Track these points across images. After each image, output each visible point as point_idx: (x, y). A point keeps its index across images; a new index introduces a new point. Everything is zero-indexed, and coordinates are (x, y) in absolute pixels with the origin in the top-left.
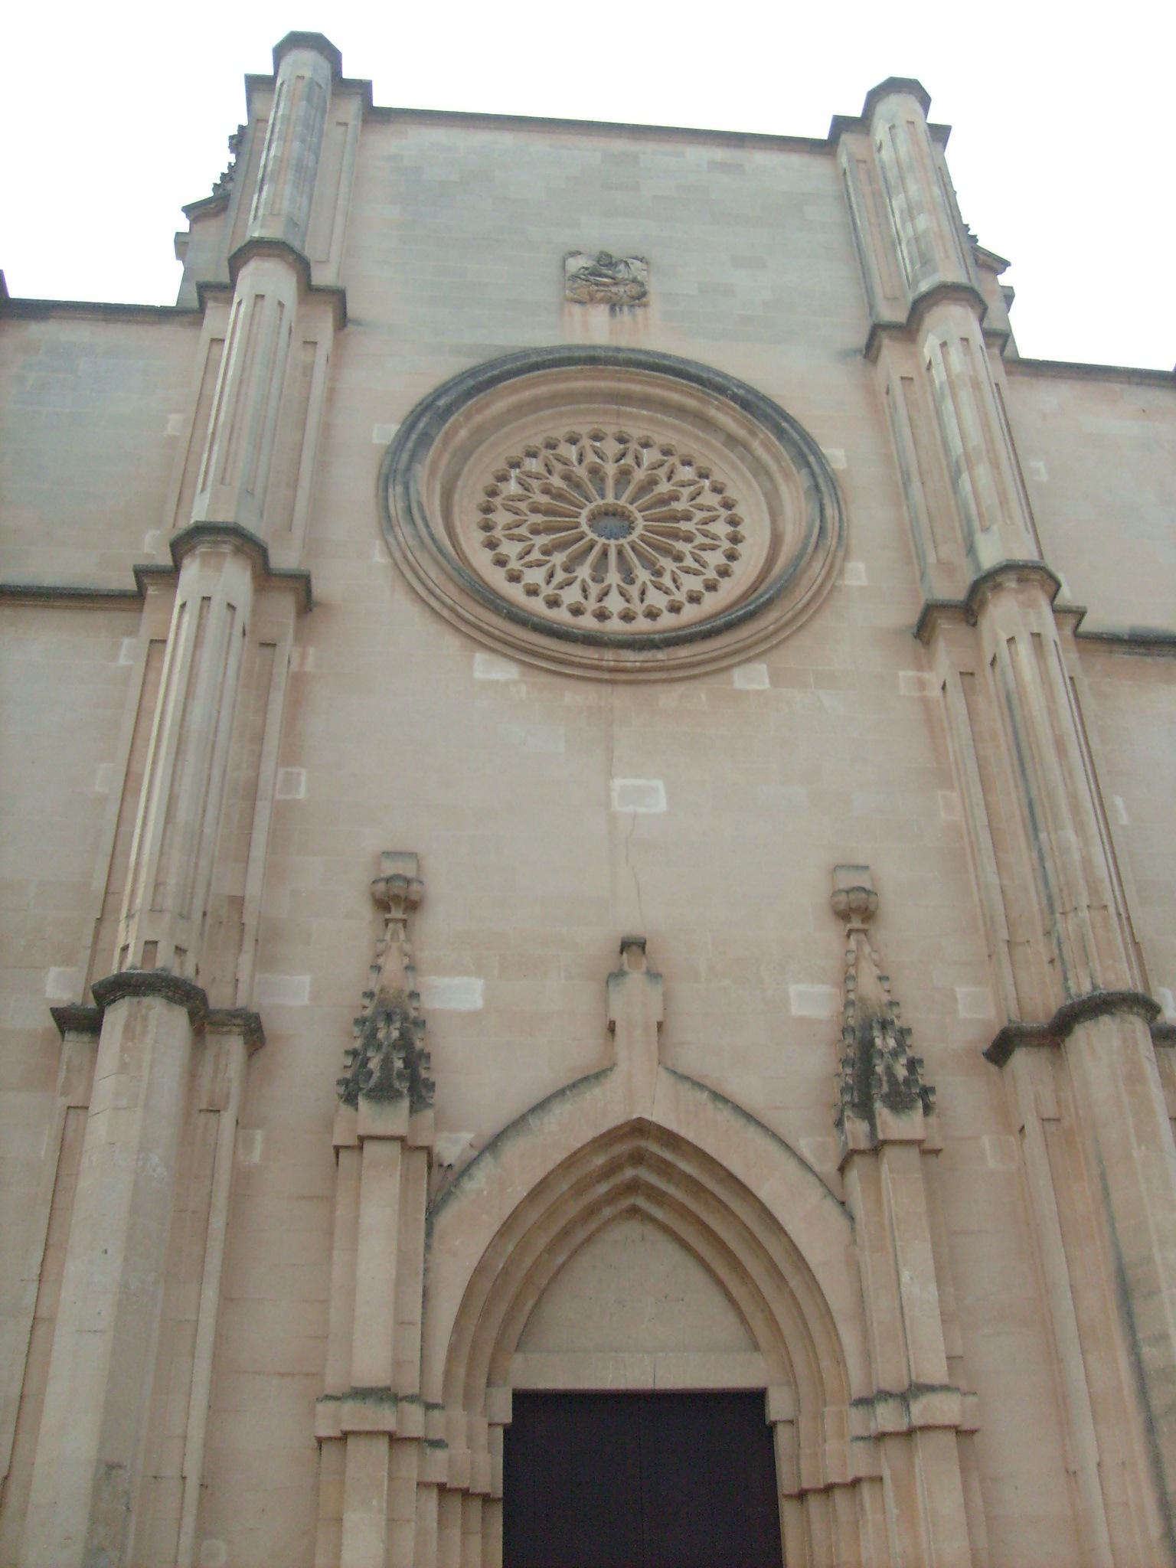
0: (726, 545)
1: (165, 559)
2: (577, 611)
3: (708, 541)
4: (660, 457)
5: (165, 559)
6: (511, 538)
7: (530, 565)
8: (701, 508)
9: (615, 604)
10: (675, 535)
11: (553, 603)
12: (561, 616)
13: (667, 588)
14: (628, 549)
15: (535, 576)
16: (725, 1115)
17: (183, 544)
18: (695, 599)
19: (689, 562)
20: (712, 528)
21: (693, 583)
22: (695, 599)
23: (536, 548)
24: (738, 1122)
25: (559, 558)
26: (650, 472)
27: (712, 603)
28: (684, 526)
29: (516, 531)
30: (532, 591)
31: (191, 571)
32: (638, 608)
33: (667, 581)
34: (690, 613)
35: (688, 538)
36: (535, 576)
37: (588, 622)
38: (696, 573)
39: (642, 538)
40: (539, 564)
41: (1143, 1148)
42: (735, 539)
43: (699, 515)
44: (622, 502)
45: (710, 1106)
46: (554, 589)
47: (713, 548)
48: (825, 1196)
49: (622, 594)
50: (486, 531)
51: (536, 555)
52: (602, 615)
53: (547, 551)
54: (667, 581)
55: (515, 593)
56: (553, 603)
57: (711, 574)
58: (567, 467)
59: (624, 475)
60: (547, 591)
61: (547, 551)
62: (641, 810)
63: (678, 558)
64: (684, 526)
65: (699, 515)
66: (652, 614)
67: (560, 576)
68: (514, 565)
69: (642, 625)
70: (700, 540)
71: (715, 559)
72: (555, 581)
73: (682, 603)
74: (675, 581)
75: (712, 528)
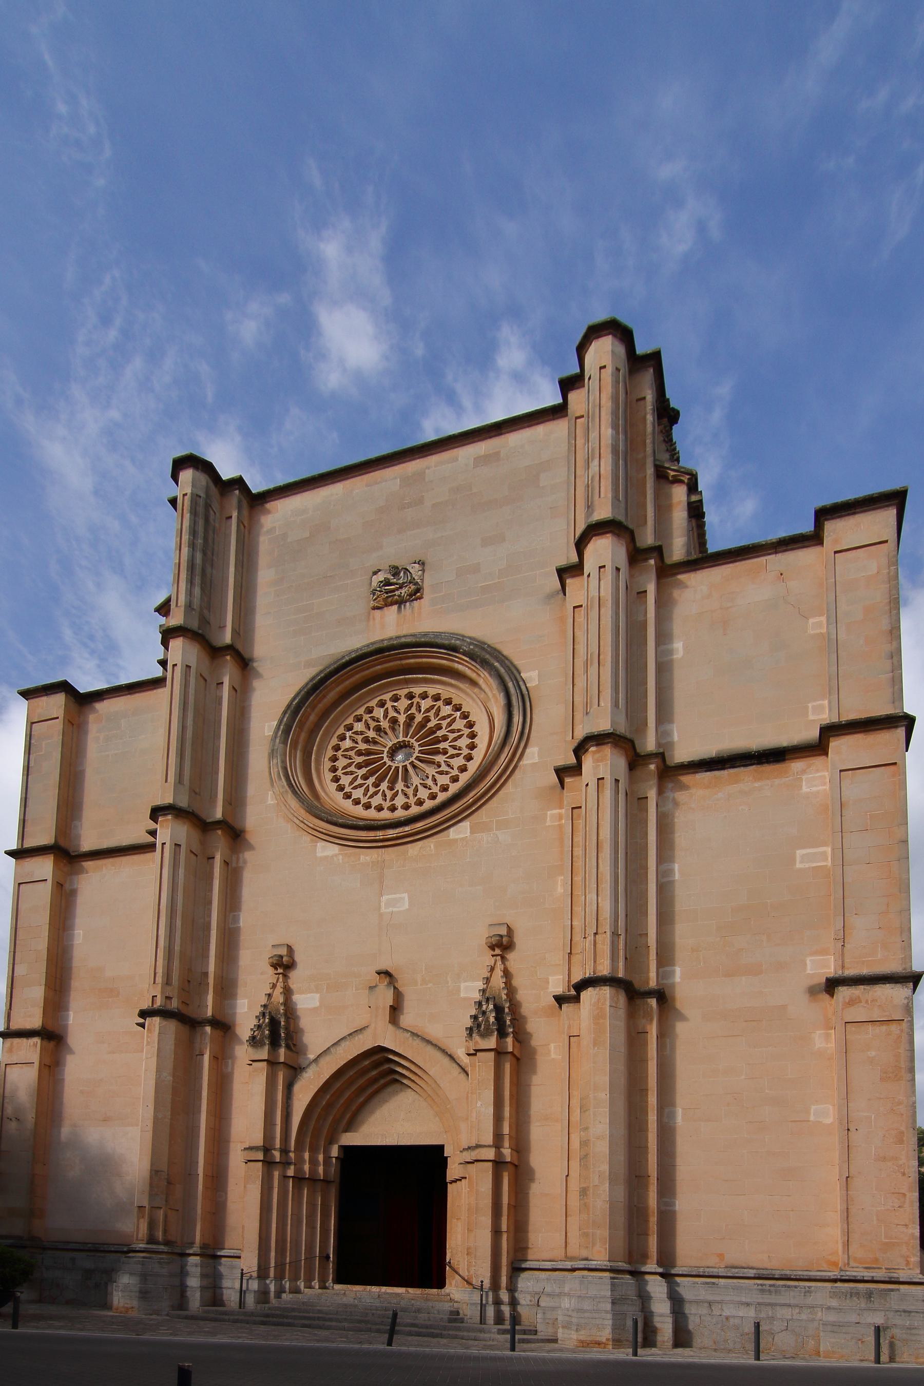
0: (467, 731)
1: (572, 760)
2: (433, 797)
3: (456, 735)
4: (382, 710)
5: (572, 760)
6: (355, 788)
7: (371, 797)
8: (444, 718)
9: (423, 794)
10: (367, 764)
11: (393, 809)
12: (400, 814)
13: (446, 771)
14: (417, 763)
15: (377, 800)
16: (417, 1042)
17: (580, 750)
18: (463, 769)
19: (451, 751)
20: (454, 726)
21: (458, 762)
22: (463, 769)
23: (370, 786)
24: (422, 1045)
25: (384, 786)
26: (387, 719)
27: (473, 767)
28: (440, 733)
29: (356, 784)
30: (380, 809)
31: (588, 763)
32: (435, 789)
33: (444, 768)
34: (464, 778)
35: (445, 738)
36: (377, 800)
37: (415, 810)
38: (458, 755)
39: (420, 752)
40: (376, 793)
41: (596, 1048)
42: (470, 725)
43: (444, 723)
44: (401, 739)
45: (411, 1038)
46: (390, 802)
47: (460, 737)
48: (460, 1073)
49: (426, 787)
50: (342, 792)
51: (372, 790)
52: (420, 803)
53: (376, 785)
54: (444, 768)
55: (372, 814)
56: (393, 809)
57: (465, 751)
58: (364, 736)
59: (378, 729)
60: (387, 804)
61: (376, 785)
62: (395, 909)
63: (445, 752)
64: (440, 733)
65: (444, 723)
66: (445, 789)
67: (389, 794)
68: (364, 800)
69: (442, 797)
70: (451, 736)
71: (464, 742)
72: (388, 798)
73: (458, 775)
74: (449, 766)
75: (454, 726)
